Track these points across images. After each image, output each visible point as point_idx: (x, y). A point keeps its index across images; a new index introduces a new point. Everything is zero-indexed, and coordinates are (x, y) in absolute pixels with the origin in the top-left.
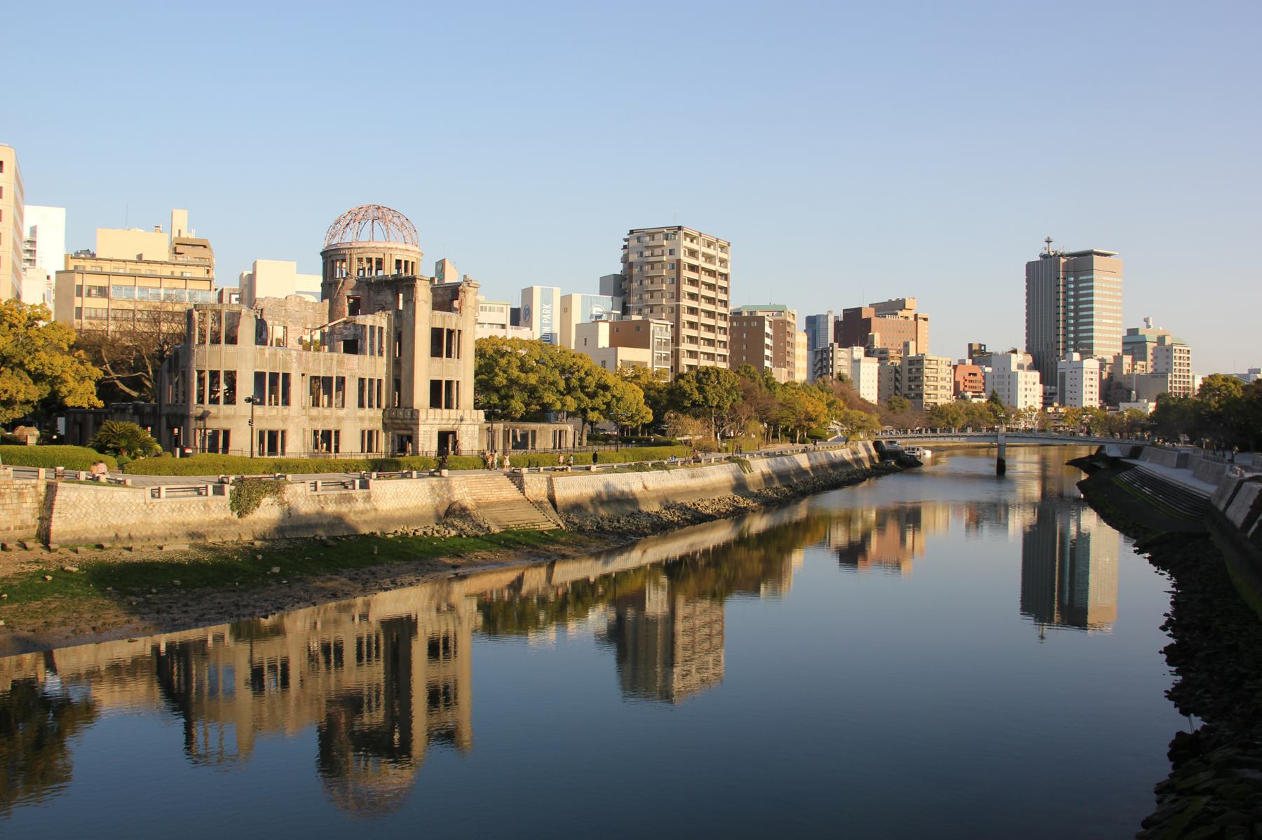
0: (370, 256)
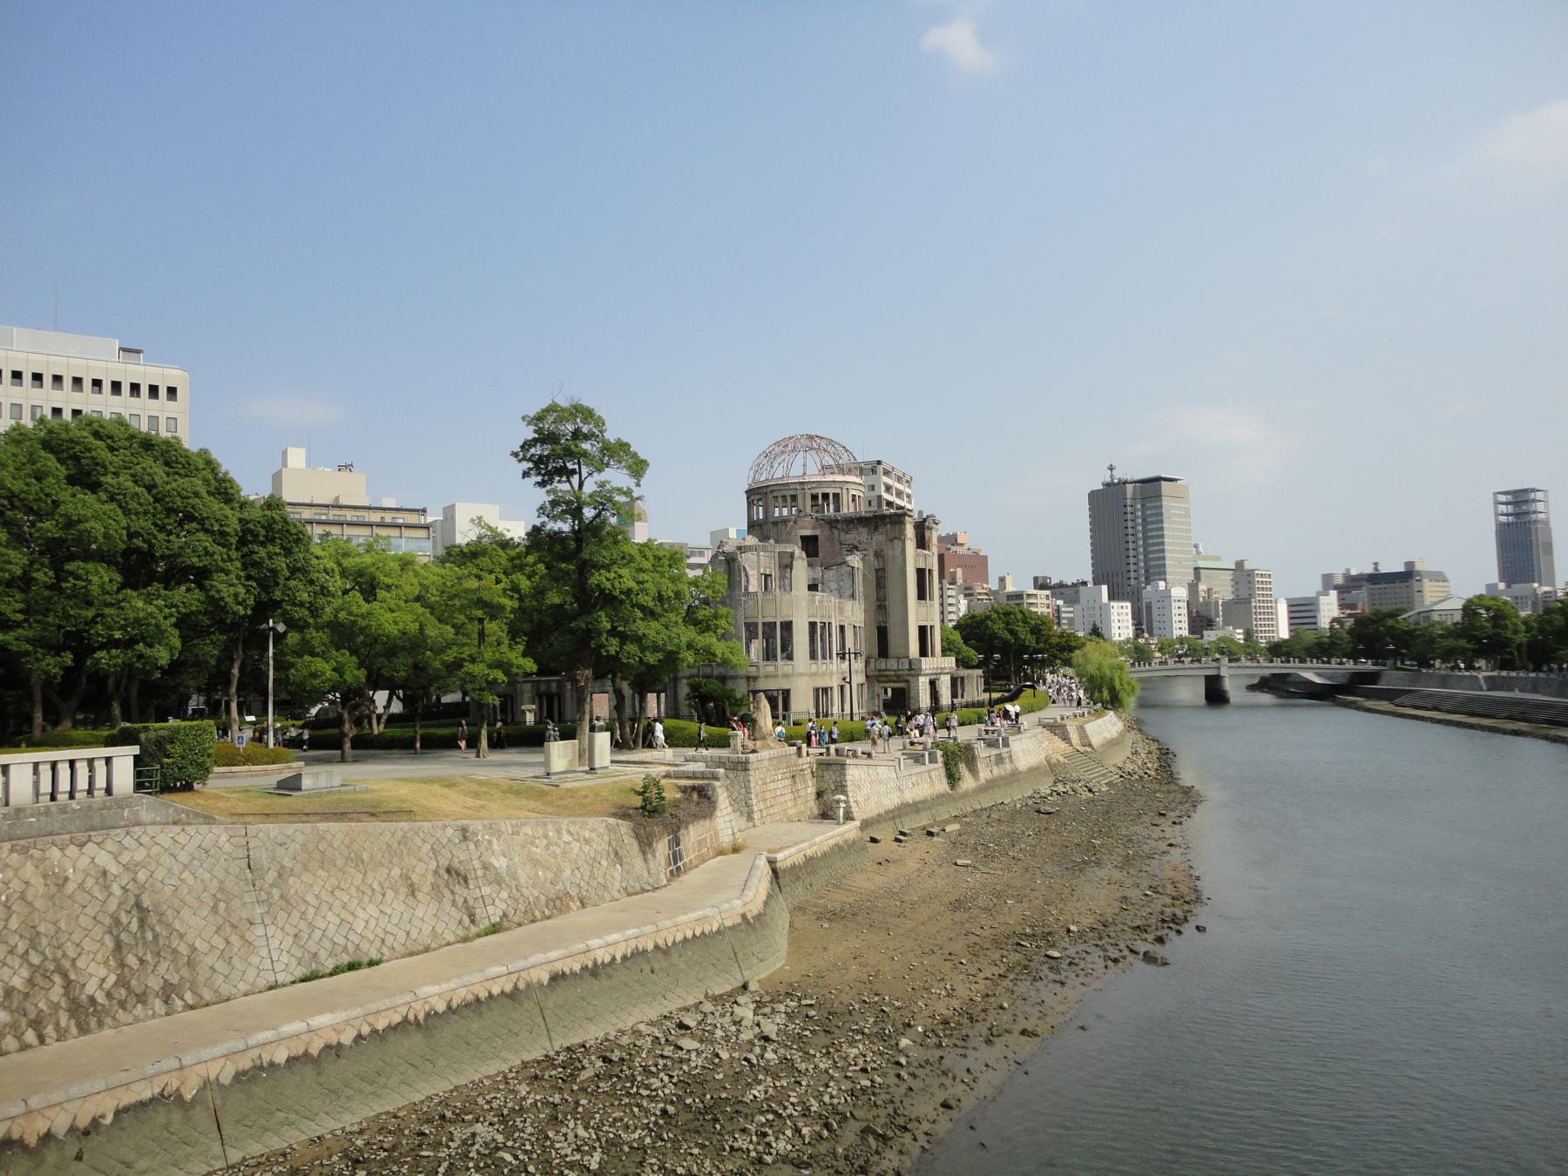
0: (827, 491)
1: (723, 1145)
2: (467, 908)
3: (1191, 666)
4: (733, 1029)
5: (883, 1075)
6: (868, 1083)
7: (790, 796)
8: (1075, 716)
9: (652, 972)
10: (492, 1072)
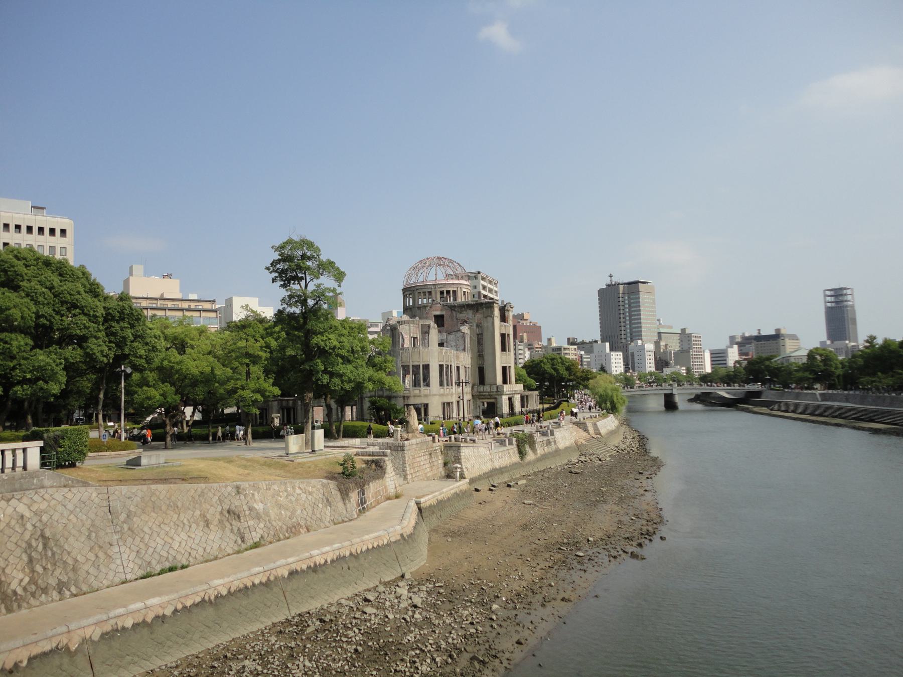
0: (449, 289)
1: (390, 669)
2: (240, 533)
3: (657, 388)
4: (396, 601)
5: (483, 626)
6: (474, 631)
7: (429, 465)
8: (591, 417)
9: (349, 569)
10: (255, 629)
